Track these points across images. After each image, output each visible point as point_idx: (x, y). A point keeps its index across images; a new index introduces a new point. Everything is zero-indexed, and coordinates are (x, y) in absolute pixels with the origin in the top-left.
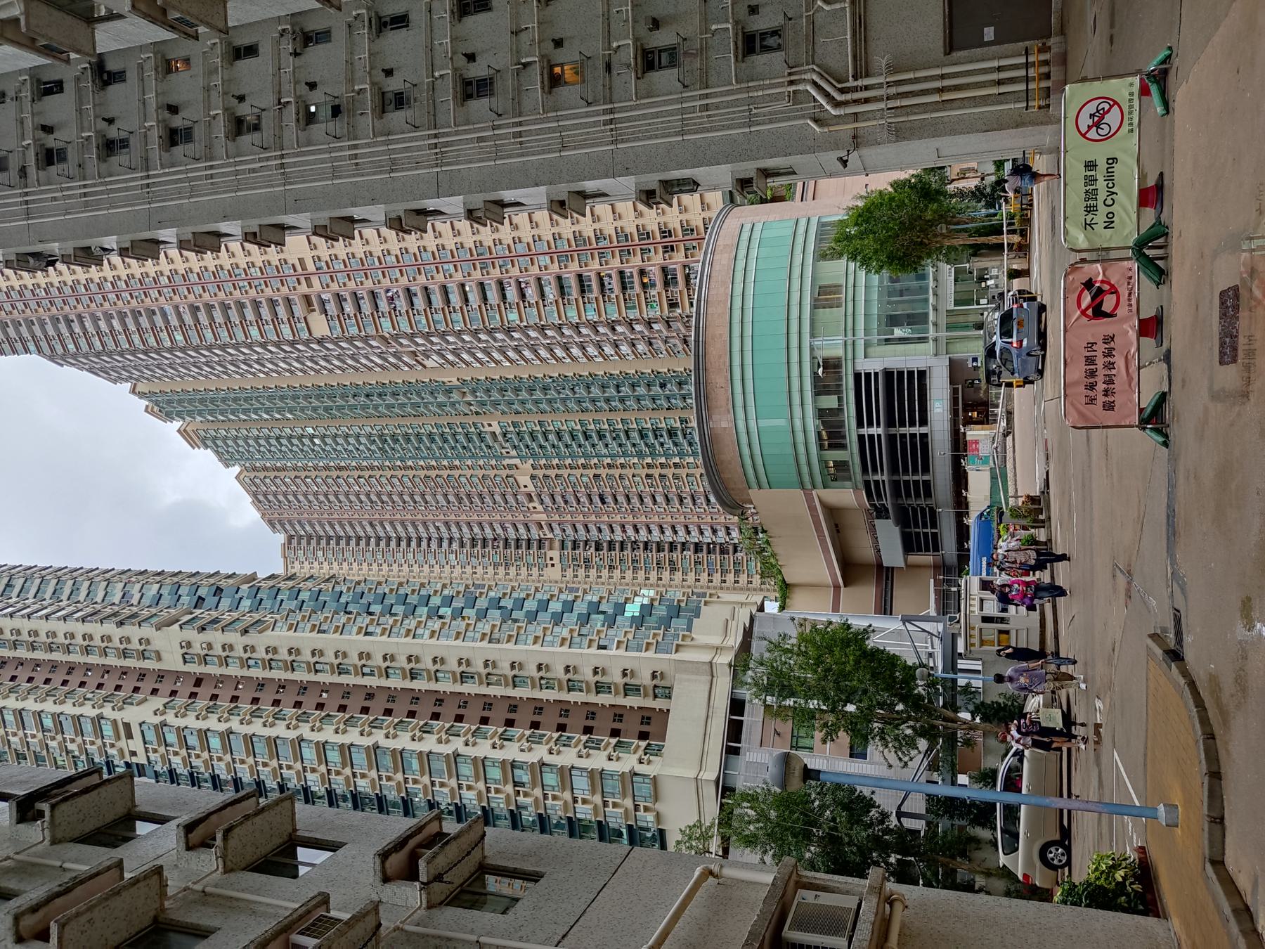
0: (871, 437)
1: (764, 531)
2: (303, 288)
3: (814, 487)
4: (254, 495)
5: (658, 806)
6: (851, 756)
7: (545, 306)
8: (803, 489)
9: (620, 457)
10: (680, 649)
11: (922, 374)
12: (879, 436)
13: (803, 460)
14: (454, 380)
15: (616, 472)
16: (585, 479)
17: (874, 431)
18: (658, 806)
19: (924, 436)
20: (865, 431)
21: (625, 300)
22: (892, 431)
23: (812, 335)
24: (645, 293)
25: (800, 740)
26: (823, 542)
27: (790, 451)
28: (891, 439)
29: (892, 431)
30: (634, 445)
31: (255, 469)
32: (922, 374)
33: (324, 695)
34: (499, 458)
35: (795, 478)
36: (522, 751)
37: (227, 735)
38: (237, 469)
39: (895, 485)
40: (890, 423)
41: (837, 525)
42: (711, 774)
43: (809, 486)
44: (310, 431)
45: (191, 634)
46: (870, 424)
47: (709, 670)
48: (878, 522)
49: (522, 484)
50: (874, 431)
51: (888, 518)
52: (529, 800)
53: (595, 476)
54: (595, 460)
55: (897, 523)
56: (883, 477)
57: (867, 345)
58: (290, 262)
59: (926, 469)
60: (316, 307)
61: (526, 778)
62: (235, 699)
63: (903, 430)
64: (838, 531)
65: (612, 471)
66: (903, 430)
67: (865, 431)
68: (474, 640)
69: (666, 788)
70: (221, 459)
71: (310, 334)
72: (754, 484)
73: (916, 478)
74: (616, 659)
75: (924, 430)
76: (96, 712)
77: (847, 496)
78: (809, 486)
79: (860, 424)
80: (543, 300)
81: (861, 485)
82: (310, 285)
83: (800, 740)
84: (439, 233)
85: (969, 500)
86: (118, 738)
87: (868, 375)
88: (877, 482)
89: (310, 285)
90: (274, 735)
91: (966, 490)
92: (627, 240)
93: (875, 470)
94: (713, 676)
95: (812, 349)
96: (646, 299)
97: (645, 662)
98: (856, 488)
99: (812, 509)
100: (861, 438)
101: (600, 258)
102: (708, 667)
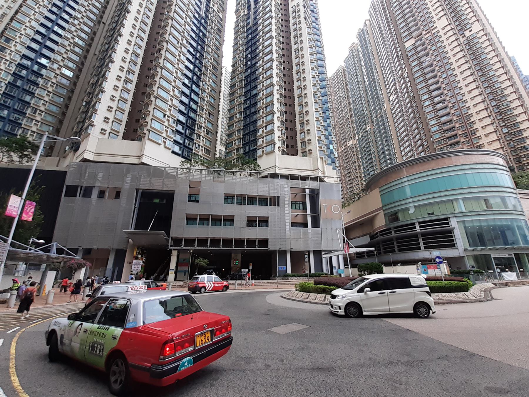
0: (415, 228)
1: (359, 198)
3: (384, 211)
4: (336, 72)
5: (265, 155)
6: (292, 223)
8: (383, 207)
10: (321, 159)
11: (453, 246)
12: (416, 230)
13: (397, 204)
14: (386, 108)
15: (357, 168)
16: (354, 159)
17: (418, 229)
18: (265, 155)
19: (419, 248)
20: (417, 224)
21: (443, 139)
22: (420, 236)
23: (463, 199)
24: (448, 146)
25: (294, 205)
26: (357, 219)
27: (396, 199)
28: (416, 235)
29: (420, 236)
30: (368, 170)
31: (344, 70)
32: (453, 246)
33: (288, 70)
34: (358, 133)
35: (387, 202)
36: (277, 108)
38: (343, 64)
39: (391, 240)
40: (423, 235)
41: (363, 224)
42: (278, 172)
43: (384, 208)
44: (359, 77)
46: (420, 227)
48: (369, 236)
49: (350, 142)
50: (418, 229)
51: (370, 240)
52: (261, 113)
53: (355, 162)
54: (360, 160)
55: (369, 243)
56: (393, 234)
57: (464, 222)
58: (435, 24)
59: (400, 250)
60: (417, 39)
61: (268, 110)
63: (421, 240)
64: (360, 225)
65: (357, 166)
66: (421, 240)
67: (417, 224)
68: (313, 89)
69: (271, 157)
70: (346, 59)
73: (381, 249)
74: (314, 136)
75: (422, 248)
76: (275, 59)
77: (381, 222)
78: (384, 208)
79: (420, 223)
81: (388, 227)
83: (294, 205)
85: (397, 266)
87: (448, 223)
88: (391, 232)
90: (274, 94)
91: (401, 265)
92: (472, 134)
93: (395, 231)
94: (313, 171)
95: (457, 200)
97: (314, 146)
98: (386, 225)
99: (373, 212)
100: (414, 224)
101: (461, 126)
102: (316, 168)
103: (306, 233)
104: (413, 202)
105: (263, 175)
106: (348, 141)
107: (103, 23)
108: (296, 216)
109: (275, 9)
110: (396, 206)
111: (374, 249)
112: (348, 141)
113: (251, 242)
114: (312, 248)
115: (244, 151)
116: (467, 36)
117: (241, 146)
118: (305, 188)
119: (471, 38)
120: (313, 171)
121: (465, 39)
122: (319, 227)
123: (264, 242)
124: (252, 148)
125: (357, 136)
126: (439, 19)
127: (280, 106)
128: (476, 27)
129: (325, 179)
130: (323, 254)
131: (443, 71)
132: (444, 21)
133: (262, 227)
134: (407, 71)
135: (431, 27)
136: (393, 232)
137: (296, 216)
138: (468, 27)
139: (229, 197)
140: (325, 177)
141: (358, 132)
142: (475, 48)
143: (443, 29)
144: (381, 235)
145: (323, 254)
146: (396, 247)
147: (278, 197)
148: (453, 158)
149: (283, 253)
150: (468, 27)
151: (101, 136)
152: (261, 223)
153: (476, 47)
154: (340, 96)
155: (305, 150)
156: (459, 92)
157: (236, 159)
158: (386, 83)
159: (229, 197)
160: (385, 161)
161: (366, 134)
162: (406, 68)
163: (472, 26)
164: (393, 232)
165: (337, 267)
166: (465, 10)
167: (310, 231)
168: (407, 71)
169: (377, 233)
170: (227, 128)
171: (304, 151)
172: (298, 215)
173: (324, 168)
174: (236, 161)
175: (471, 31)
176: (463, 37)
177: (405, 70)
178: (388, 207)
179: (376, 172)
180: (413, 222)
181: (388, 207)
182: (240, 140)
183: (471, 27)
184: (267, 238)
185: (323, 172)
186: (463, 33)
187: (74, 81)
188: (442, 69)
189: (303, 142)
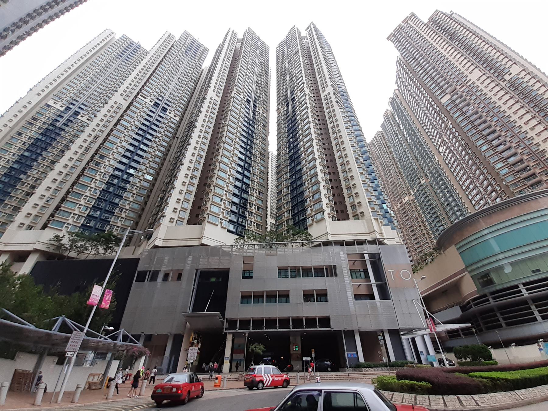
1: (433, 260)
2: (458, 87)
3: (469, 272)
5: (315, 224)
7: (497, 155)
8: (467, 267)
9: (428, 223)
10: (376, 220)
15: (421, 224)
16: (414, 215)
18: (315, 224)
21: (519, 181)
26: (437, 285)
30: (435, 225)
34: (412, 188)
35: (471, 262)
37: (314, 159)
41: (446, 291)
42: (331, 238)
43: (469, 269)
45: (332, 92)
47: (371, 231)
49: (405, 198)
51: (462, 311)
55: (462, 316)
61: (313, 180)
62: (314, 93)
64: (443, 292)
69: (322, 224)
71: (440, 99)
72: (458, 246)
74: (364, 198)
78: (469, 269)
80: (500, 153)
81: (482, 293)
82: (460, 88)
84: (511, 108)
86: (299, 90)
89: (460, 88)
94: (369, 233)
96: (525, 188)
97: (366, 208)
98: (478, 292)
99: (455, 275)
100: (517, 286)
102: (373, 230)
103: (374, 307)
104: (505, 258)
105: (315, 244)
106: (402, 197)
107: (177, 138)
108: (359, 286)
109: (311, 114)
110: (484, 266)
111: (470, 325)
112: (402, 197)
113: (311, 322)
114: (385, 327)
115: (294, 222)
116: (508, 80)
117: (291, 217)
118: (364, 254)
119: (513, 80)
120: (369, 233)
121: (505, 83)
122: (390, 299)
123: (325, 321)
124: (301, 218)
125: (411, 191)
126: (471, 73)
127: (325, 175)
128: (515, 70)
129: (385, 241)
130: (402, 335)
131: (492, 115)
132: (477, 73)
133: (321, 301)
134: (450, 123)
135: (464, 81)
136: (491, 300)
137: (359, 286)
138: (506, 71)
139: (282, 271)
140: (385, 239)
141: (411, 187)
142: (521, 88)
143: (478, 80)
144: (475, 305)
145: (402, 335)
146: (501, 319)
147: (335, 266)
148: (540, 200)
149: (350, 334)
150: (506, 71)
151: (170, 224)
152: (319, 298)
153: (522, 87)
154: (383, 157)
155: (357, 213)
156: (519, 130)
157: (287, 230)
158: (431, 137)
159: (282, 271)
160: (453, 213)
161: (421, 188)
162: (448, 120)
163: (510, 69)
164: (491, 300)
165: (425, 352)
166: (498, 58)
167: (378, 304)
168: (450, 123)
169: (469, 303)
170: (276, 202)
171: (355, 214)
172: (360, 285)
173: (381, 229)
174: (287, 232)
175: (511, 74)
176: (503, 82)
177: (449, 122)
178: (474, 267)
179: (446, 227)
180: (514, 284)
181: (474, 267)
182: (289, 212)
183: (509, 71)
184: (328, 315)
185: (381, 234)
186: (503, 78)
187: (153, 184)
188: (490, 113)
189: (353, 205)
